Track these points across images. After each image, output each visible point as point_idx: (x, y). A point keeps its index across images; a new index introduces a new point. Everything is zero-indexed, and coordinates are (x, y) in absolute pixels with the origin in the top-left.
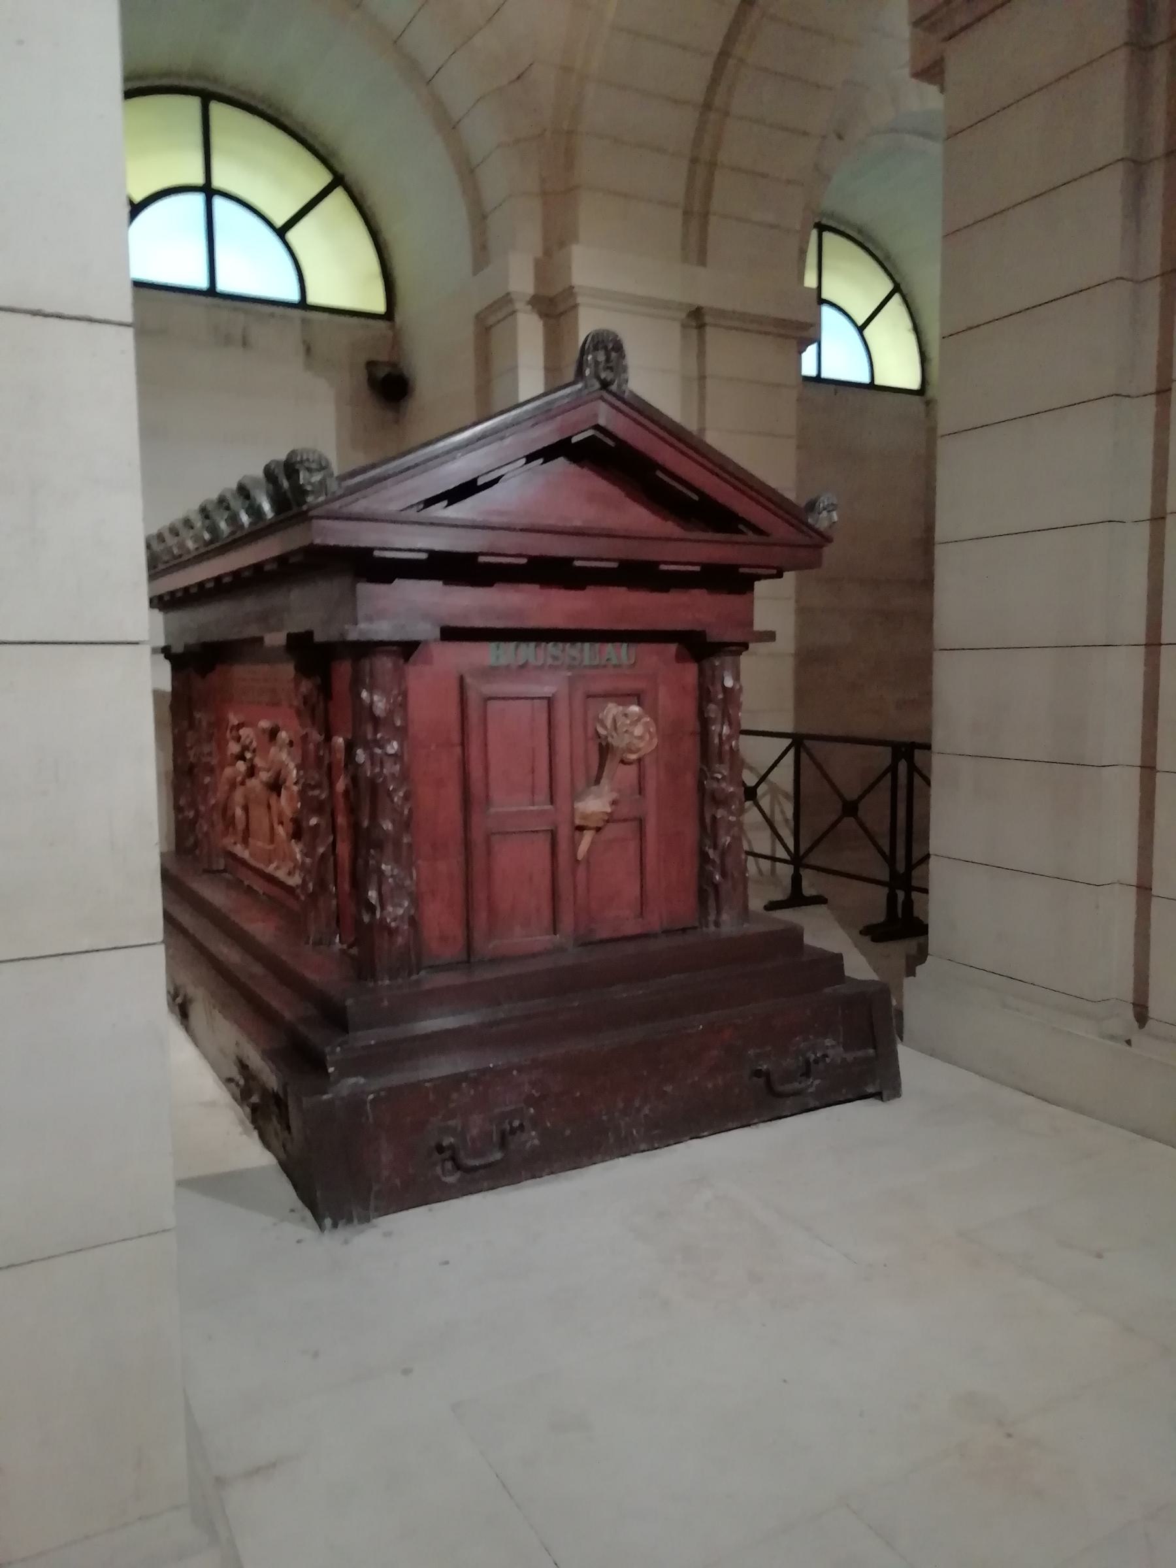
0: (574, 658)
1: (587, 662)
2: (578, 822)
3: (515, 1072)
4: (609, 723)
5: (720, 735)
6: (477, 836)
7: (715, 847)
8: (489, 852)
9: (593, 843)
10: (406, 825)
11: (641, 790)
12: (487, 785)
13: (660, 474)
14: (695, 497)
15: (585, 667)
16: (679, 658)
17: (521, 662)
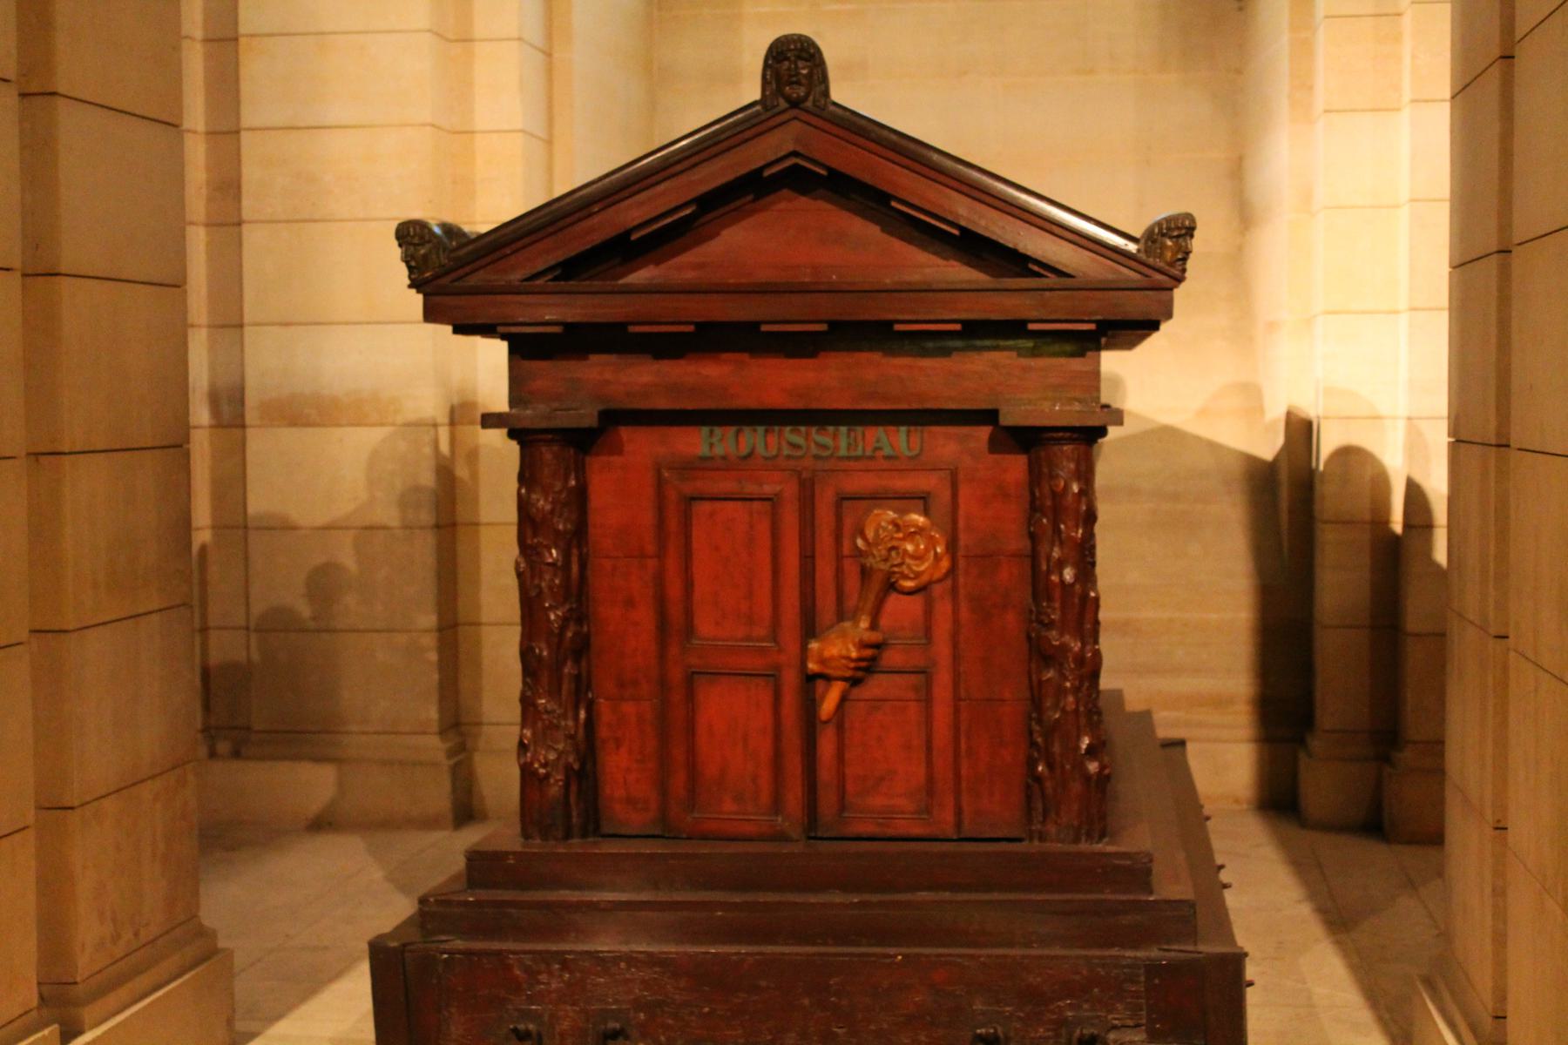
0: (824, 447)
1: (843, 452)
2: (812, 666)
3: (623, 965)
4: (870, 534)
5: (1049, 557)
6: (676, 675)
7: (1040, 721)
8: (690, 694)
9: (844, 699)
10: (581, 649)
11: (928, 632)
12: (689, 614)
13: (893, 204)
14: (956, 232)
15: (841, 458)
16: (995, 445)
17: (745, 451)
